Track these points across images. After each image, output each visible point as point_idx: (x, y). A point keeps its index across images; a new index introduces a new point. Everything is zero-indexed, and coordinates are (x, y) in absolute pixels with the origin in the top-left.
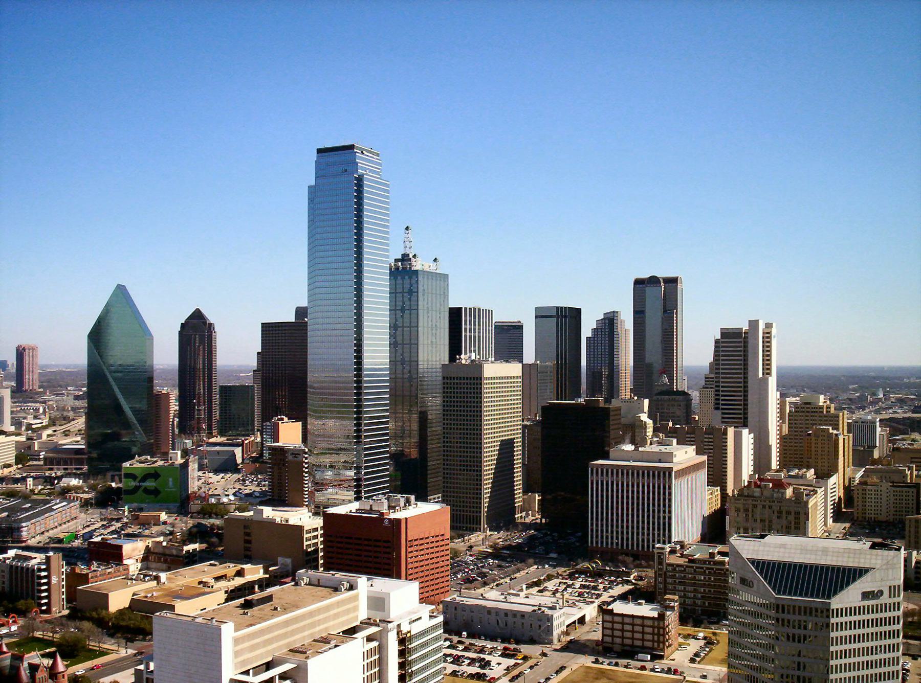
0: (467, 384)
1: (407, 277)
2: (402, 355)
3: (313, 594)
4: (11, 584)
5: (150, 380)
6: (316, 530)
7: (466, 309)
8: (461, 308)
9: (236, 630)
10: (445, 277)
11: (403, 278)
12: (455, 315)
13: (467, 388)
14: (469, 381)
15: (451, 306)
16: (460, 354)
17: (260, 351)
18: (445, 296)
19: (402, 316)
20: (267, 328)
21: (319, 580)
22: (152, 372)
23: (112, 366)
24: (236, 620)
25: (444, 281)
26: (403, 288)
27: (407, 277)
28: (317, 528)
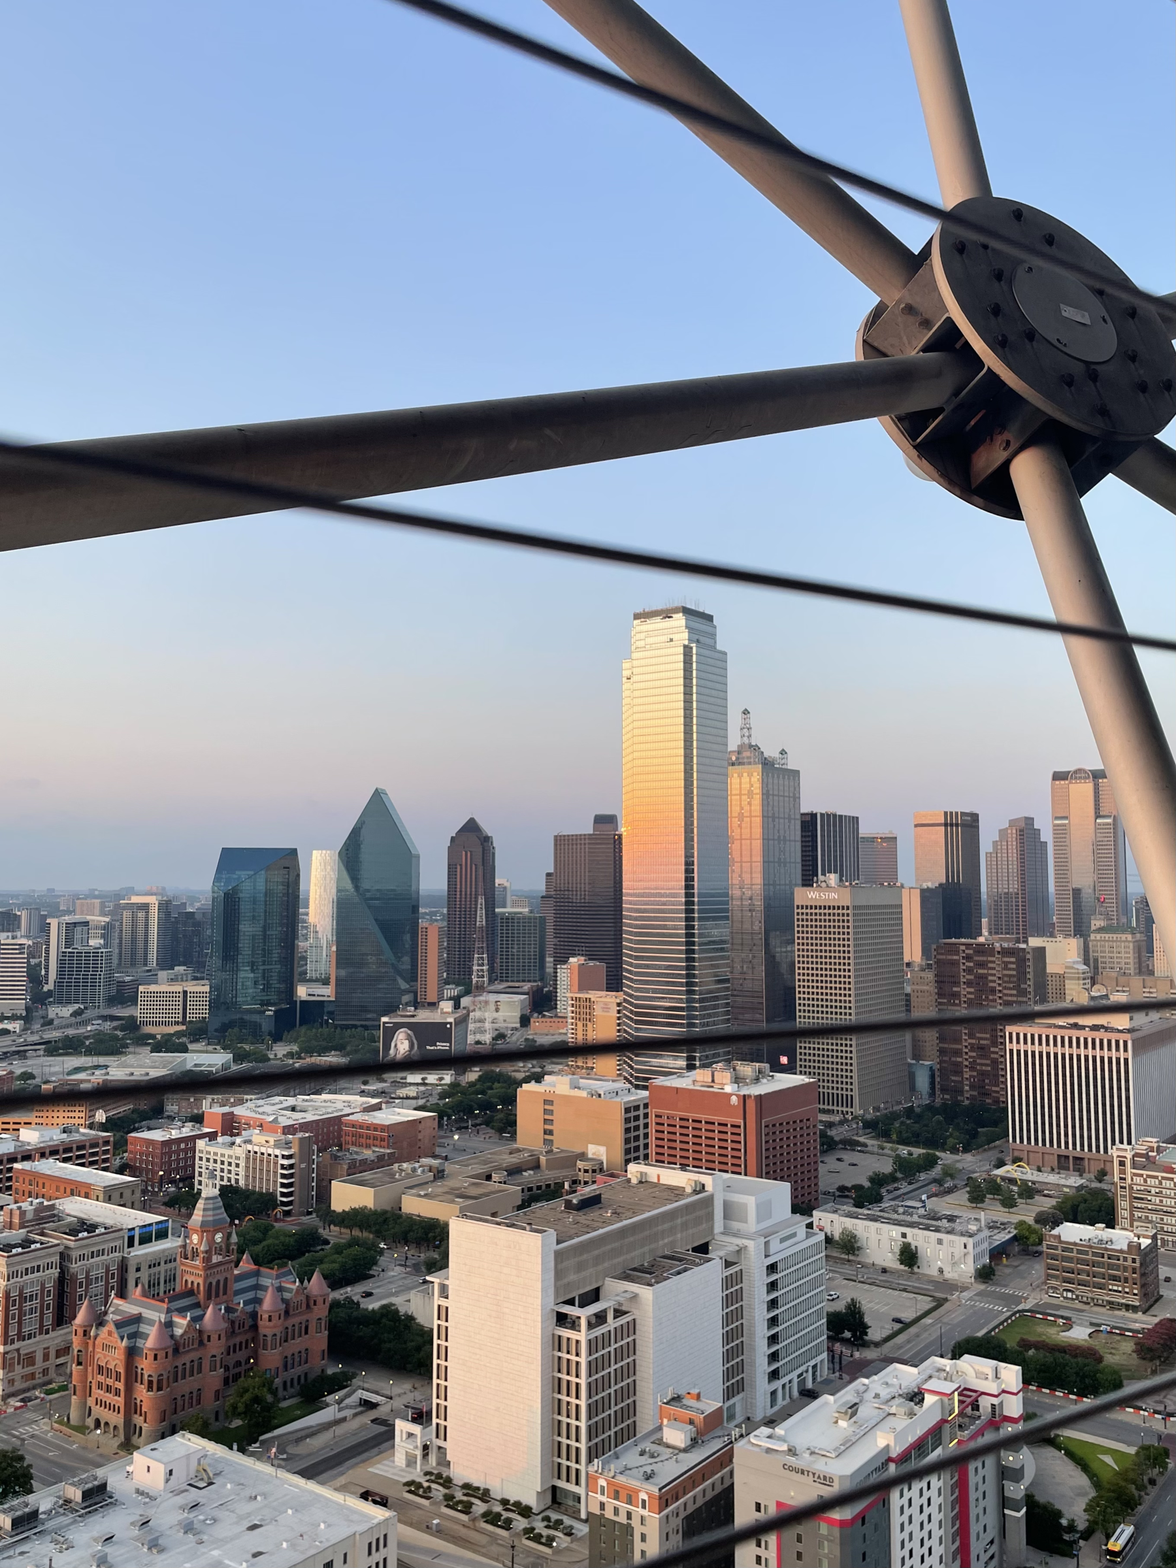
0: (829, 914)
1: (745, 775)
2: (740, 876)
3: (653, 1195)
4: (247, 1177)
5: (415, 909)
6: (637, 1108)
7: (822, 815)
8: (816, 814)
9: (558, 1242)
10: (796, 773)
11: (740, 776)
12: (809, 823)
13: (825, 920)
14: (831, 911)
15: (803, 810)
16: (817, 876)
17: (552, 870)
18: (796, 798)
19: (740, 826)
20: (561, 842)
21: (659, 1177)
22: (418, 900)
23: (368, 891)
24: (556, 1227)
25: (794, 779)
26: (741, 788)
27: (745, 775)
28: (639, 1106)
